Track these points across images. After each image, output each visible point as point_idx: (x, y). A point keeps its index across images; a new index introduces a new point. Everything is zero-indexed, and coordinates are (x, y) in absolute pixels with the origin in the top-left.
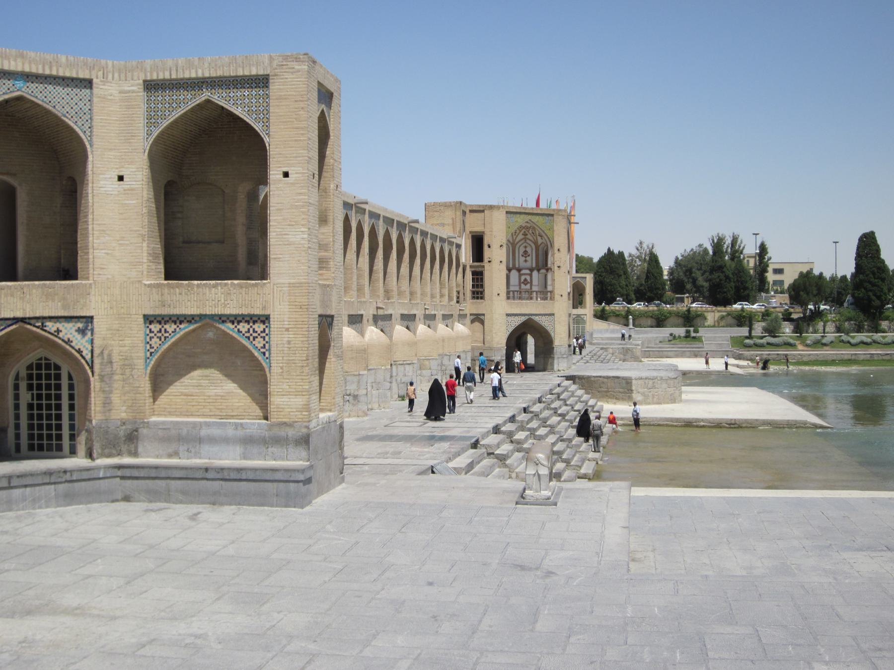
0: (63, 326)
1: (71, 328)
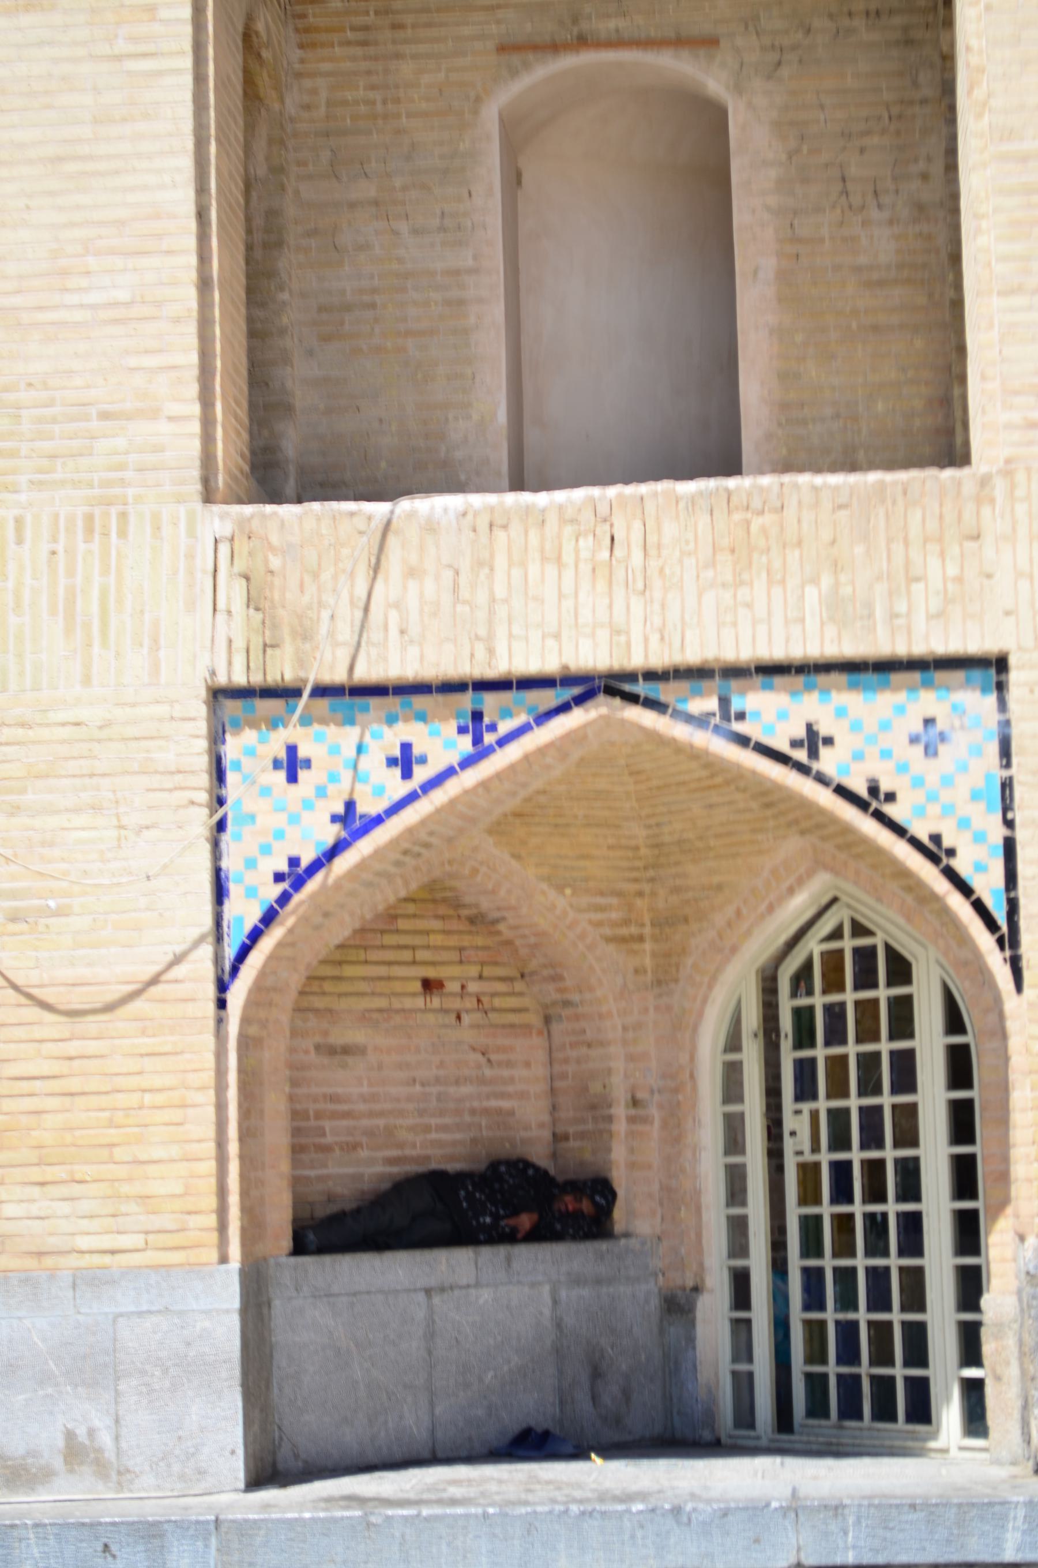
0: (841, 713)
1: (885, 726)
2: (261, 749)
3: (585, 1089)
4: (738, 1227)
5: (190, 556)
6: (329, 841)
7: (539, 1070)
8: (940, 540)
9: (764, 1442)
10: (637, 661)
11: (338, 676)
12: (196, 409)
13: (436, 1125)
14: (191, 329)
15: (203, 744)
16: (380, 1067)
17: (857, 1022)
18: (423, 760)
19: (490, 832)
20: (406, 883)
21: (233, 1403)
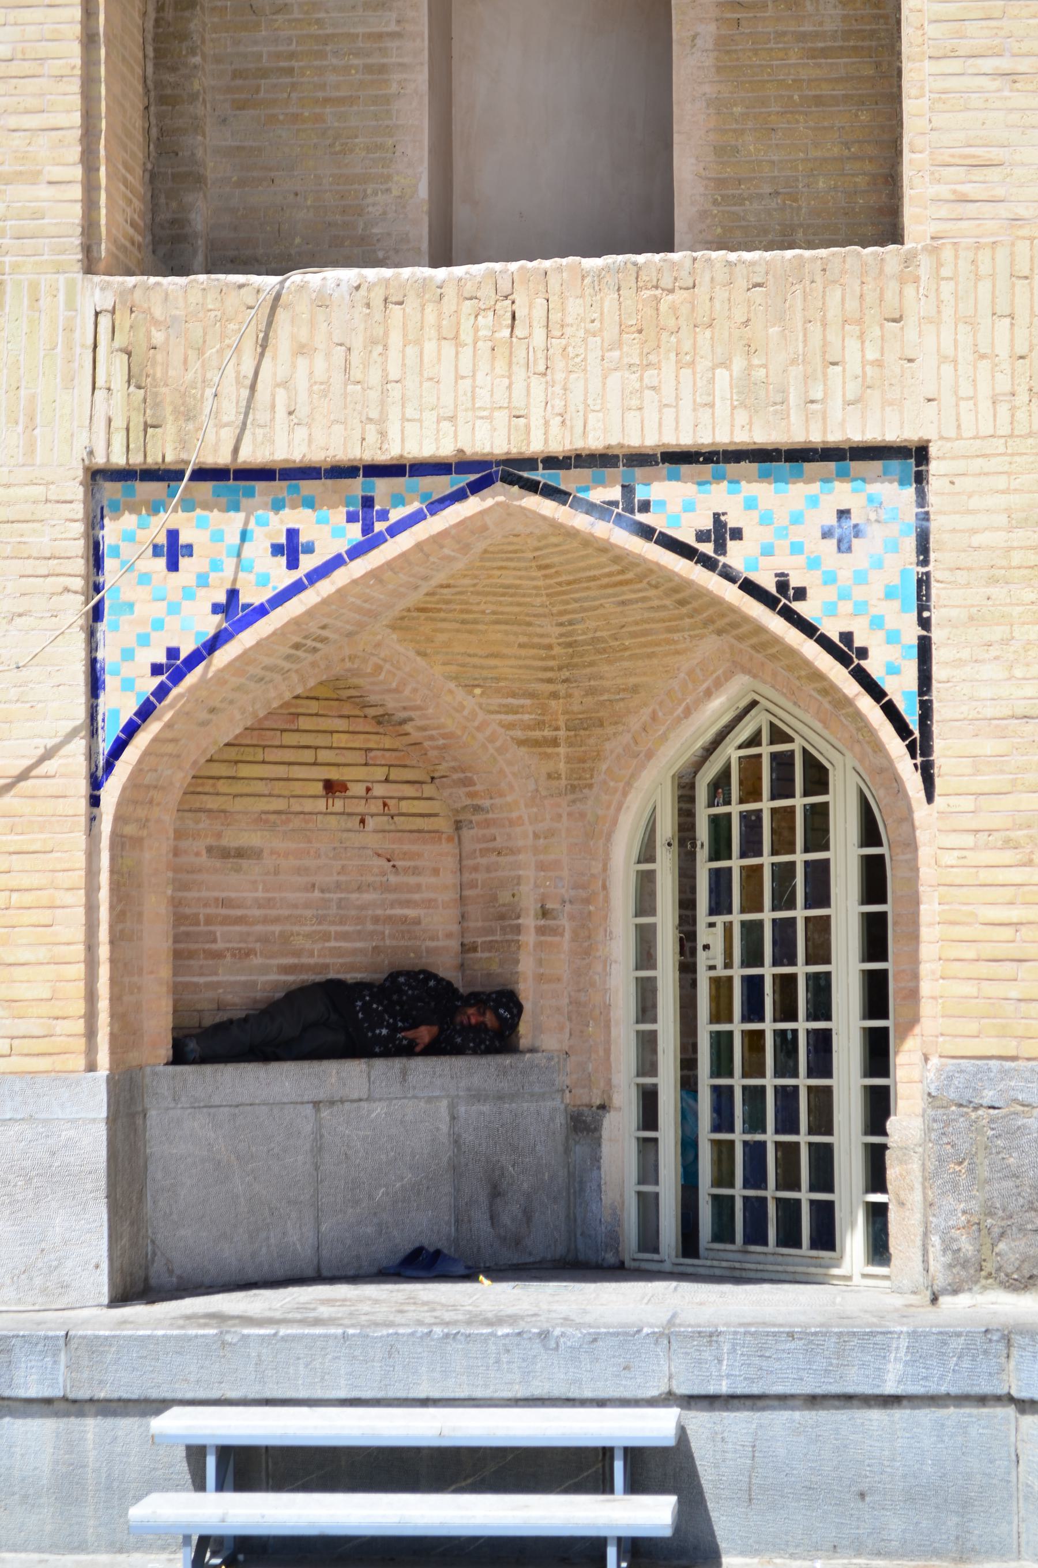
0: (750, 504)
1: (796, 519)
2: (141, 534)
3: (494, 898)
4: (648, 1043)
5: (69, 329)
6: (211, 632)
7: (448, 878)
8: (860, 322)
9: (667, 1267)
10: (536, 446)
11: (222, 458)
12: (77, 173)
13: (336, 932)
14: (74, 86)
15: (79, 528)
16: (277, 872)
17: (773, 831)
18: (310, 549)
19: (393, 628)
20: (303, 680)
21: (99, 1214)
